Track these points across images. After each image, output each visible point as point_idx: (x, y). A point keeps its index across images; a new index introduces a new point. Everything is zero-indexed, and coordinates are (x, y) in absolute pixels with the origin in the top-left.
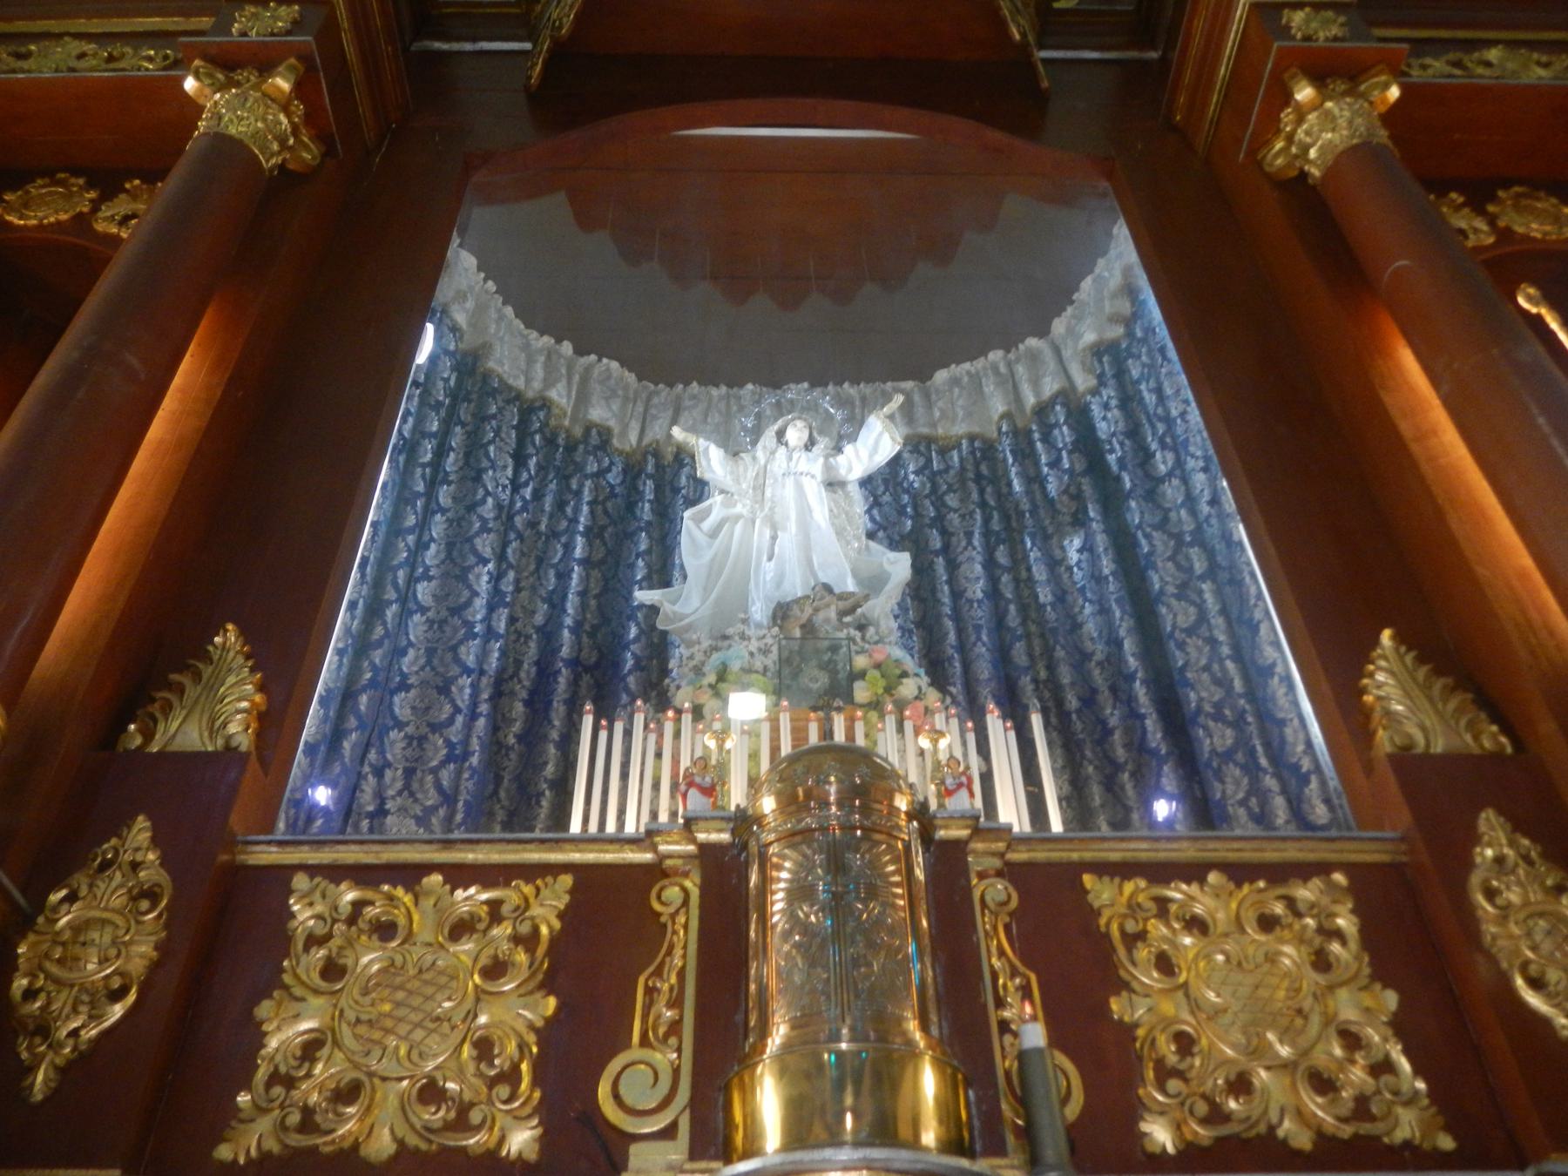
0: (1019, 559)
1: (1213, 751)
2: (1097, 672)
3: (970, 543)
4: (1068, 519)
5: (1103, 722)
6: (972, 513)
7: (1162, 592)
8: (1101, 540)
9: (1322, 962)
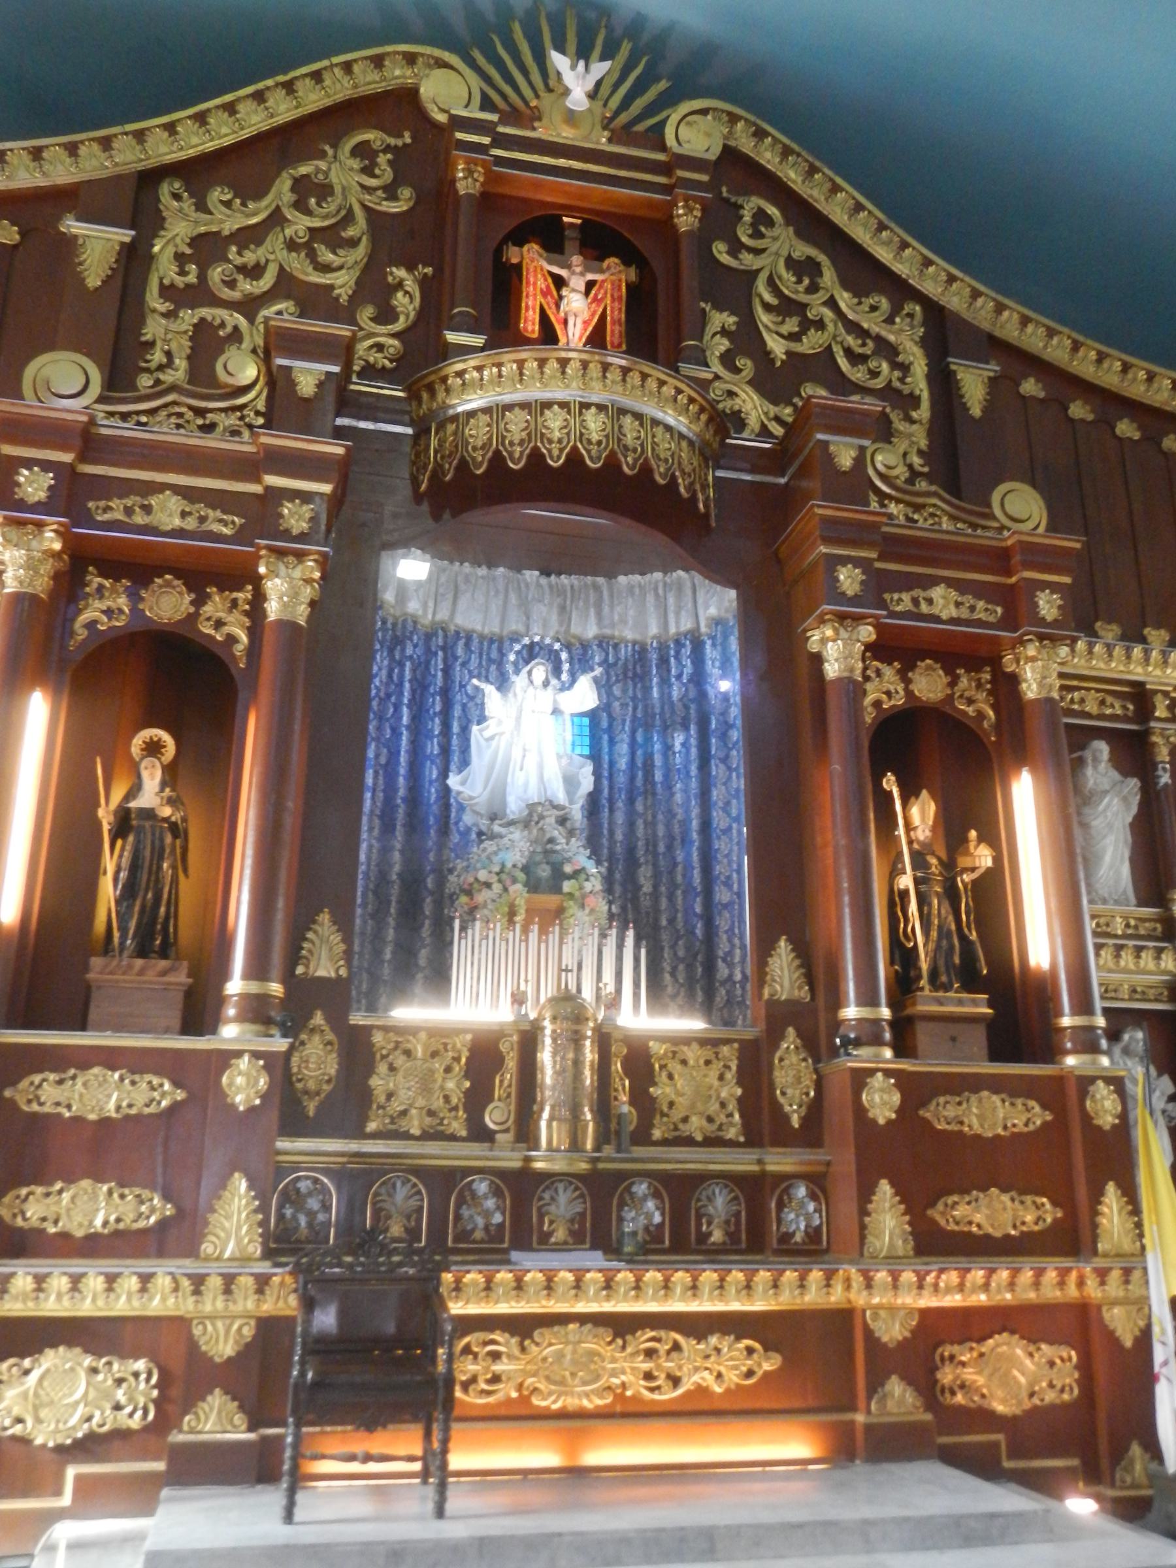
0: (648, 739)
1: (720, 903)
2: (677, 826)
3: (623, 729)
4: (679, 720)
5: (674, 858)
6: (627, 705)
7: (716, 803)
8: (693, 741)
9: (721, 1078)
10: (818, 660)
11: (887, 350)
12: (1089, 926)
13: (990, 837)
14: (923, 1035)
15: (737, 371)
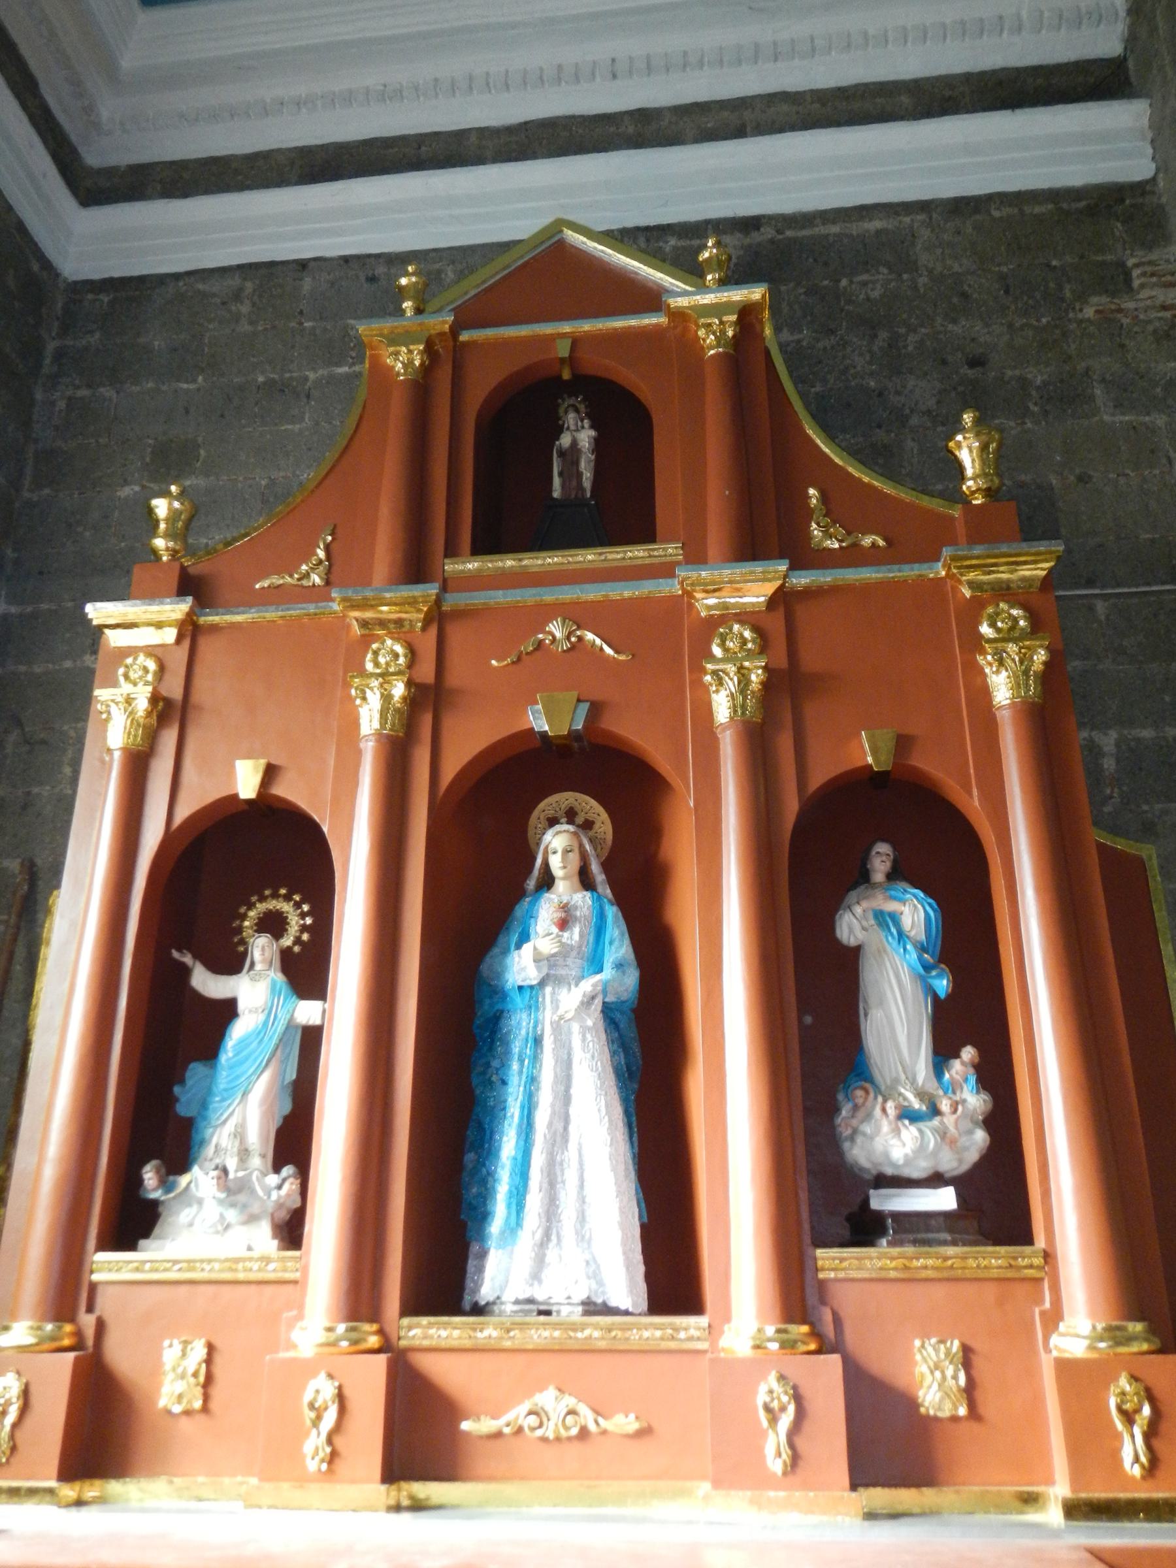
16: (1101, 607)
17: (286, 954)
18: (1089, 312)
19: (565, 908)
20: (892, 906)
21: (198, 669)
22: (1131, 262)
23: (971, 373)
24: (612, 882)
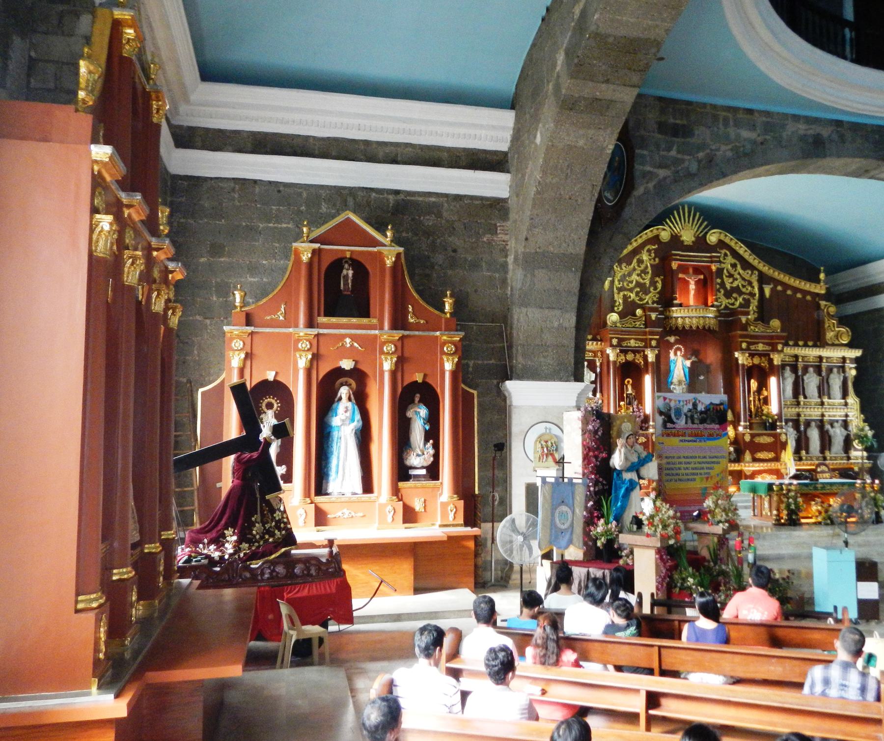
10: (737, 359)
11: (750, 283)
12: (783, 403)
13: (767, 390)
14: (755, 426)
15: (720, 292)
16: (475, 327)
17: (275, 413)
18: (485, 239)
19: (347, 408)
20: (419, 410)
21: (254, 342)
22: (498, 224)
23: (453, 254)
24: (355, 399)
